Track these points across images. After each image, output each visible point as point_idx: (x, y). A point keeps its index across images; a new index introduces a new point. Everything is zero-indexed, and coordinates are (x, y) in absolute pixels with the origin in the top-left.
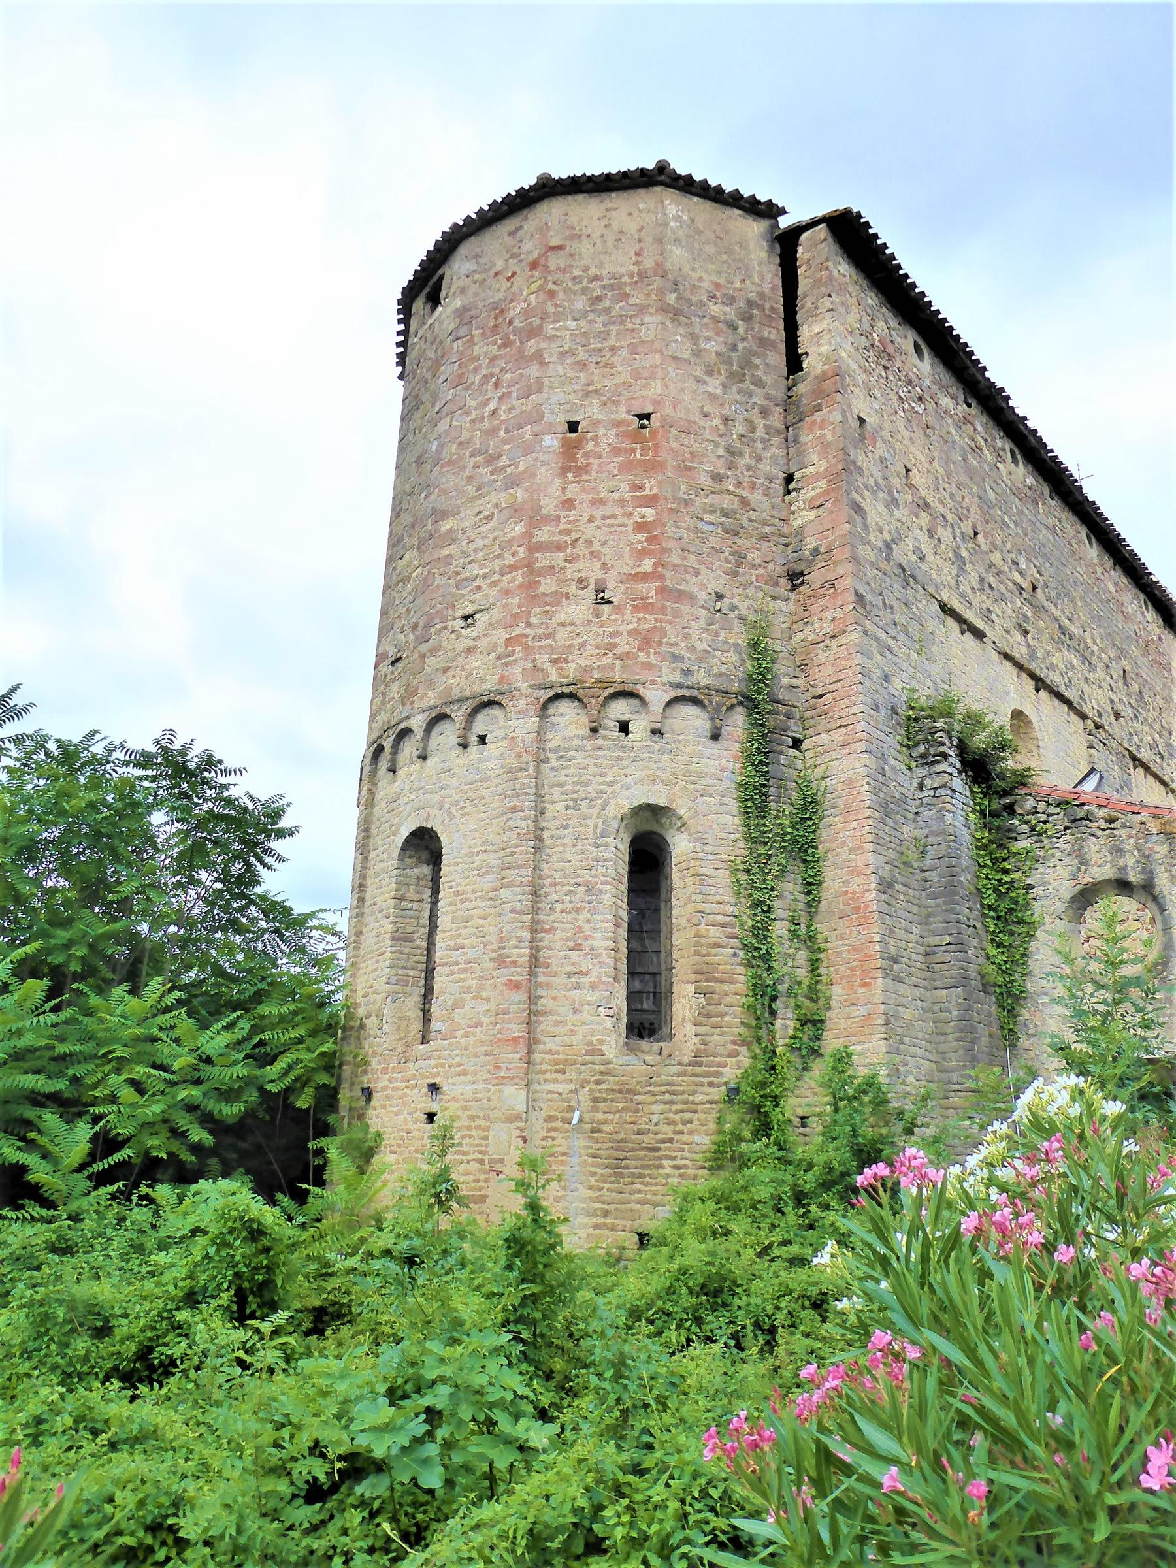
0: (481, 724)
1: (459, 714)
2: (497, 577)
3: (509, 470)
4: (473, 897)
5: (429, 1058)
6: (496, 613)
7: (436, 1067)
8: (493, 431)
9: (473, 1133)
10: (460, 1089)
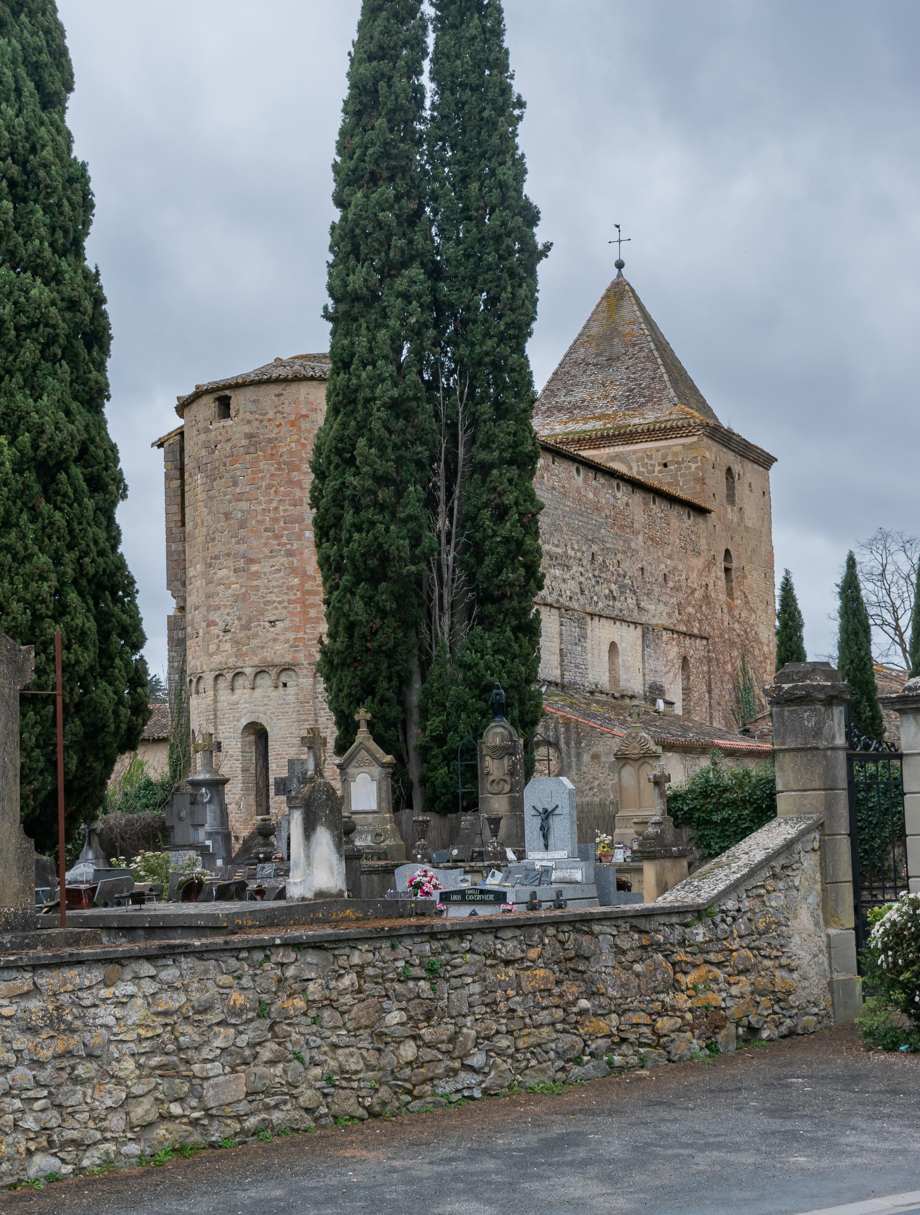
0: (284, 678)
1: (274, 672)
2: (286, 604)
6: (287, 623)
8: (275, 520)
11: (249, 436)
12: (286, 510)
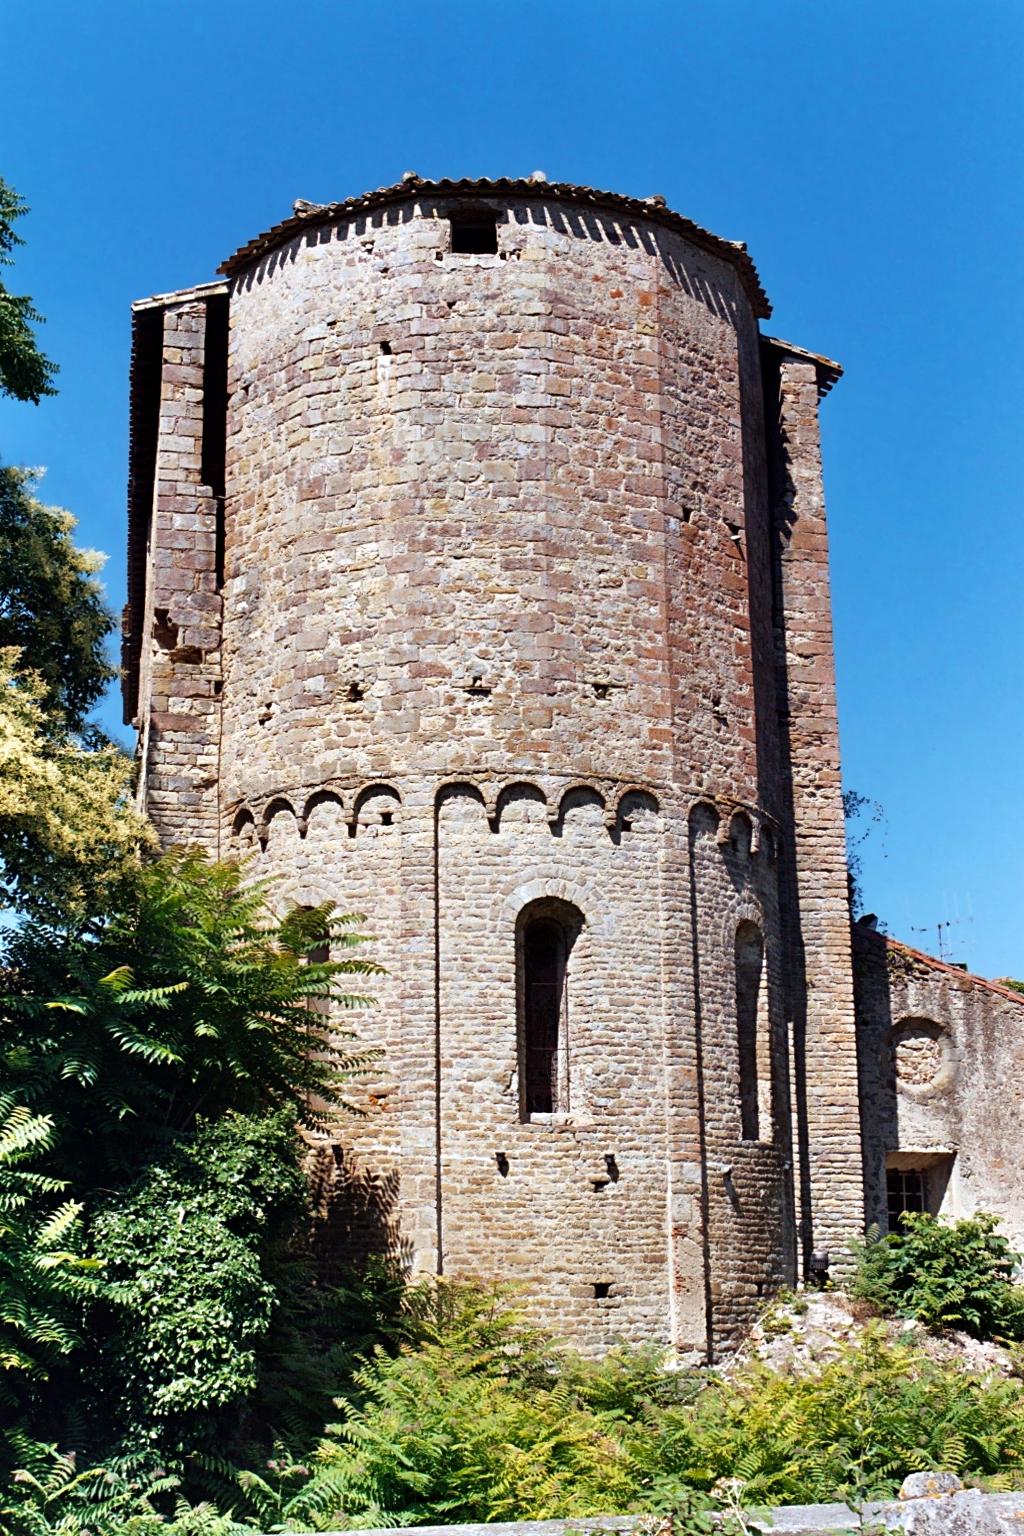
3: (636, 538)
4: (631, 983)
5: (595, 1132)
7: (604, 1140)
9: (650, 1201)
10: (634, 1162)
11: (554, 299)
12: (630, 466)
